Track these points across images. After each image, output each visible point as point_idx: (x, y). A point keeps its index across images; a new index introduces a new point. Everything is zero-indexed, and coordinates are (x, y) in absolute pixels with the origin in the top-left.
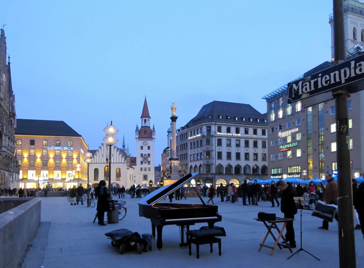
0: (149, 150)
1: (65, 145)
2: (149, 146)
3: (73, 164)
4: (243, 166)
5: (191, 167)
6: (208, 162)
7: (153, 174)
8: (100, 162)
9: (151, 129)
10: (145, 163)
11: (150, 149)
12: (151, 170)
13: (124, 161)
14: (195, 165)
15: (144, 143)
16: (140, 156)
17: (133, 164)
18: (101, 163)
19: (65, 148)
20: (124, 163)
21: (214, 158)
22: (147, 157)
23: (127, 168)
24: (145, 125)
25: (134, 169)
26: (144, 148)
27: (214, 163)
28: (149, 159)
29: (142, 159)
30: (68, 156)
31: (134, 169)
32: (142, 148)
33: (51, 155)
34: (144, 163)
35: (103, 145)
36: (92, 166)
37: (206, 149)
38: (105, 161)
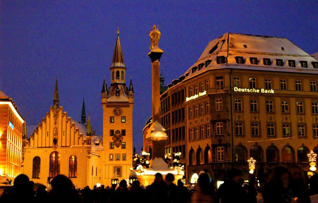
4: (280, 147)
5: (192, 150)
6: (220, 141)
7: (130, 165)
8: (44, 146)
10: (118, 147)
12: (127, 158)
14: (198, 147)
15: (115, 111)
18: (45, 147)
21: (230, 134)
22: (120, 136)
27: (231, 143)
36: (29, 152)
37: (216, 117)
38: (52, 144)
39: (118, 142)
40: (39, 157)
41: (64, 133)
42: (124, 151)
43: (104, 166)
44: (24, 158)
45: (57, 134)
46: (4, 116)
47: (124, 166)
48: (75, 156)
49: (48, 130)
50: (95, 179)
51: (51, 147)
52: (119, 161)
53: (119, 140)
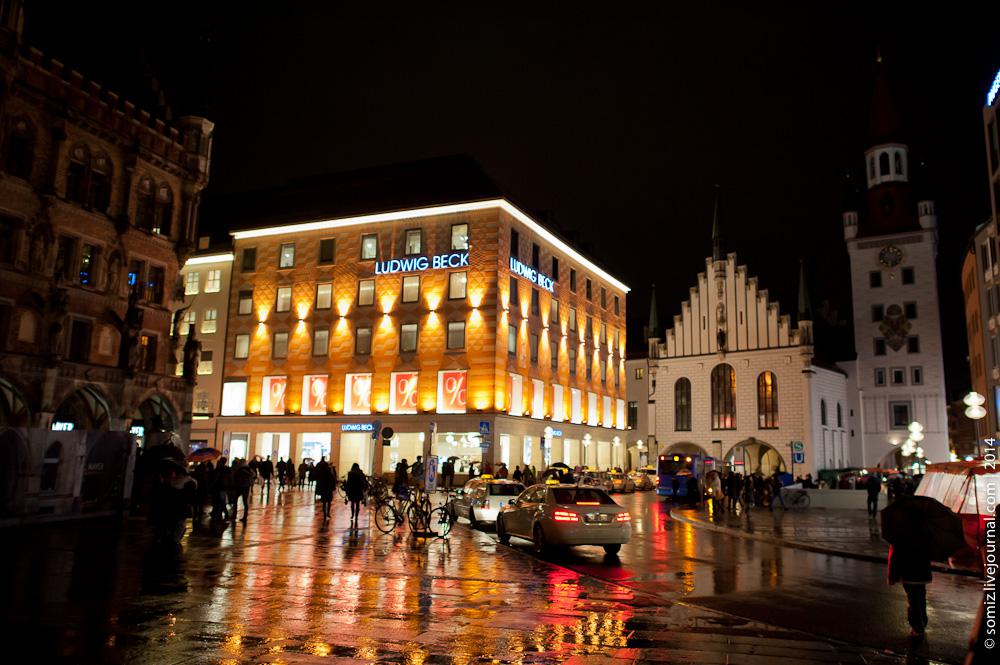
0: (908, 287)
1: (437, 248)
2: (906, 264)
3: (467, 337)
11: (917, 280)
13: (791, 335)
15: (881, 256)
19: (440, 262)
20: (790, 346)
23: (804, 372)
24: (886, 178)
25: (847, 376)
26: (884, 276)
29: (881, 328)
30: (450, 300)
33: (387, 302)
34: (889, 349)
38: (714, 349)
39: (896, 337)
40: (687, 380)
41: (741, 318)
42: (914, 360)
43: (861, 400)
44: (657, 383)
45: (723, 320)
46: (491, 241)
47: (918, 399)
48: (772, 374)
49: (704, 313)
50: (844, 434)
51: (714, 354)
52: (903, 388)
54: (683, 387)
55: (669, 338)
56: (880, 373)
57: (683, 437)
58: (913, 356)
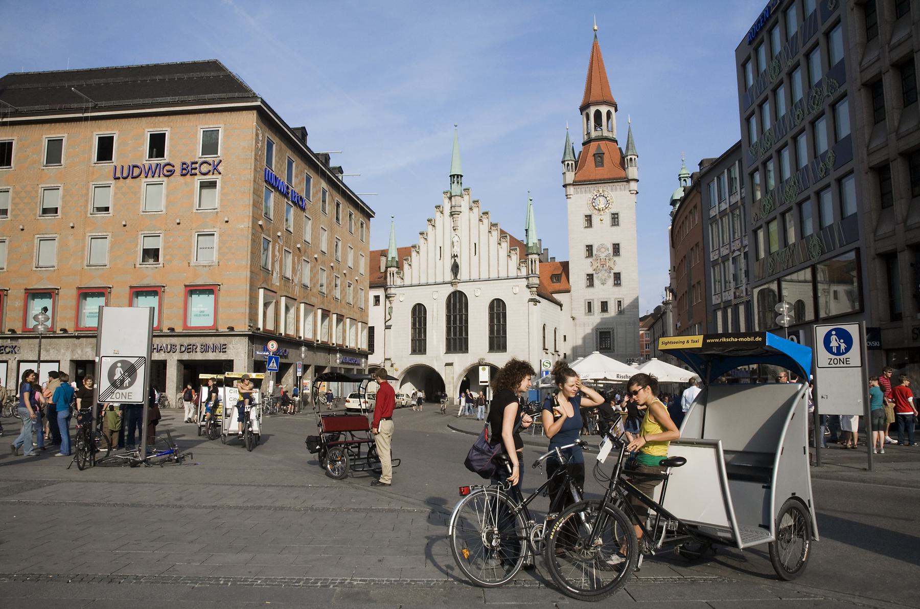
0: (615, 228)
2: (614, 211)
9: (620, 149)
13: (519, 269)
16: (583, 252)
17: (557, 286)
23: (531, 300)
24: (599, 133)
25: (561, 305)
26: (595, 220)
28: (619, 265)
31: (561, 305)
32: (589, 218)
34: (596, 282)
35: (442, 212)
38: (449, 277)
53: (605, 268)
54: (419, 313)
55: (406, 266)
56: (589, 303)
57: (419, 360)
58: (617, 289)
